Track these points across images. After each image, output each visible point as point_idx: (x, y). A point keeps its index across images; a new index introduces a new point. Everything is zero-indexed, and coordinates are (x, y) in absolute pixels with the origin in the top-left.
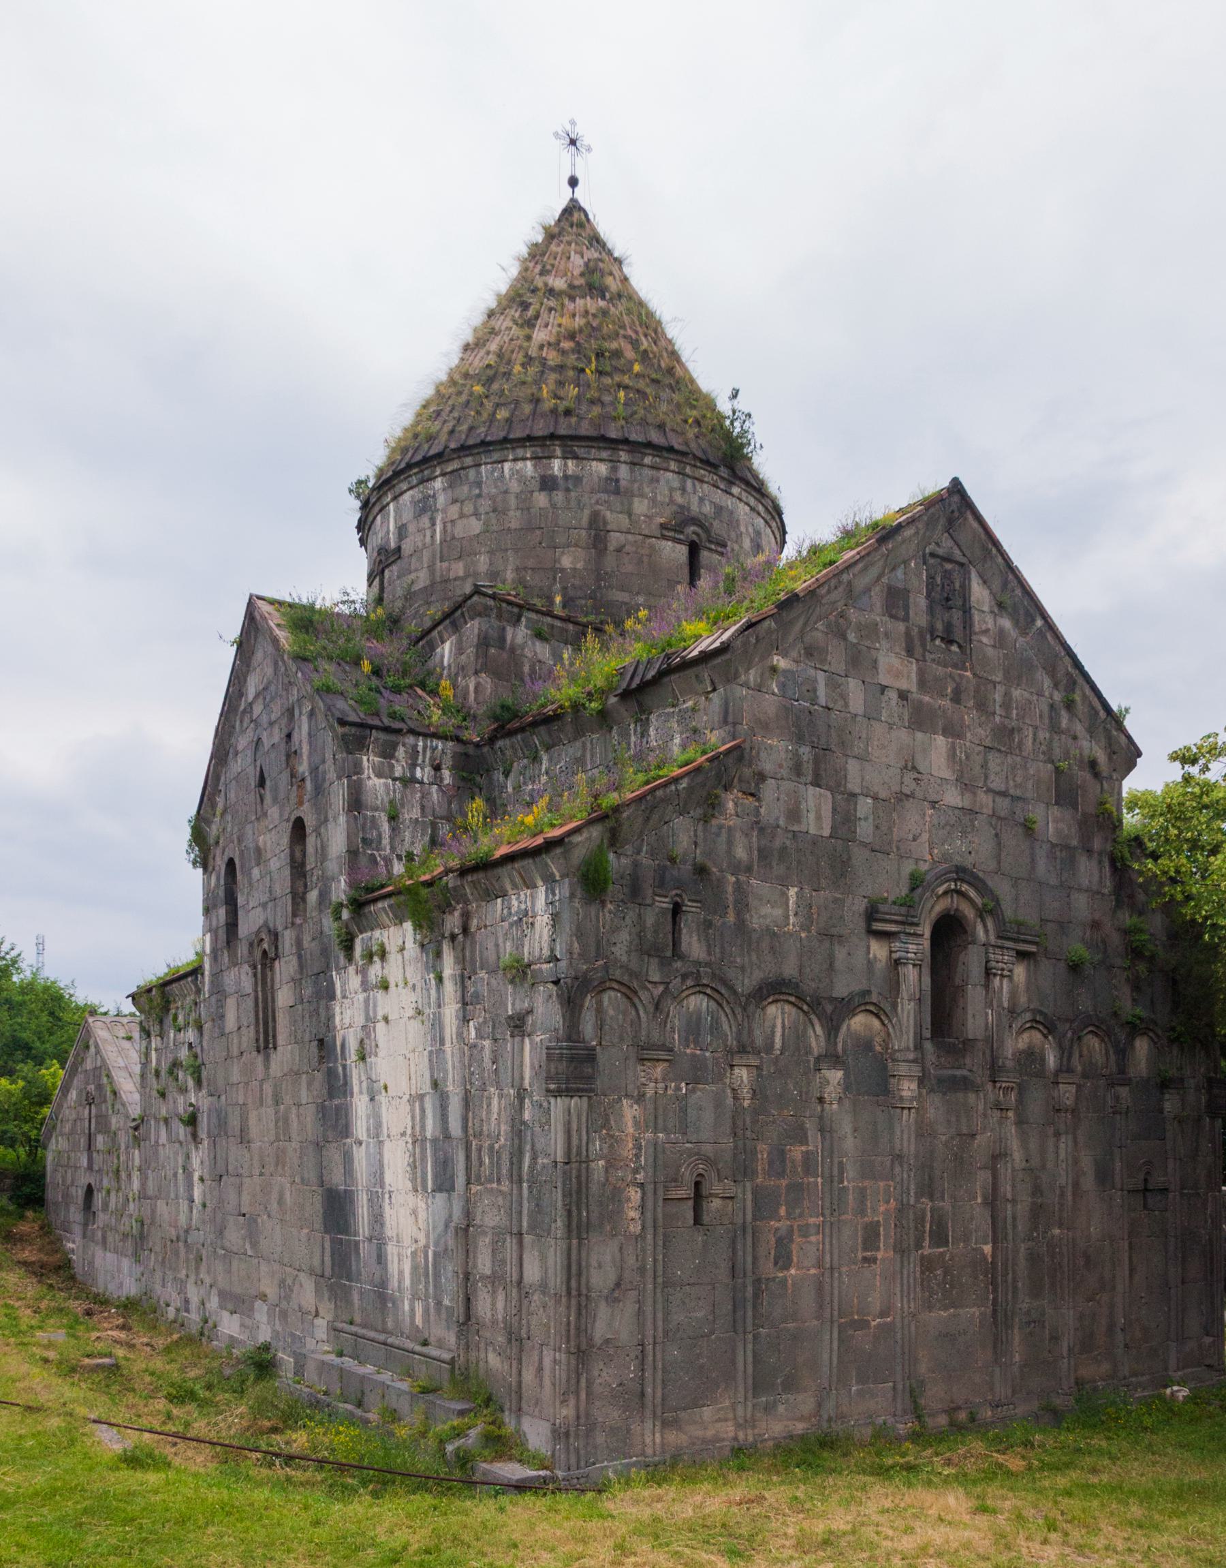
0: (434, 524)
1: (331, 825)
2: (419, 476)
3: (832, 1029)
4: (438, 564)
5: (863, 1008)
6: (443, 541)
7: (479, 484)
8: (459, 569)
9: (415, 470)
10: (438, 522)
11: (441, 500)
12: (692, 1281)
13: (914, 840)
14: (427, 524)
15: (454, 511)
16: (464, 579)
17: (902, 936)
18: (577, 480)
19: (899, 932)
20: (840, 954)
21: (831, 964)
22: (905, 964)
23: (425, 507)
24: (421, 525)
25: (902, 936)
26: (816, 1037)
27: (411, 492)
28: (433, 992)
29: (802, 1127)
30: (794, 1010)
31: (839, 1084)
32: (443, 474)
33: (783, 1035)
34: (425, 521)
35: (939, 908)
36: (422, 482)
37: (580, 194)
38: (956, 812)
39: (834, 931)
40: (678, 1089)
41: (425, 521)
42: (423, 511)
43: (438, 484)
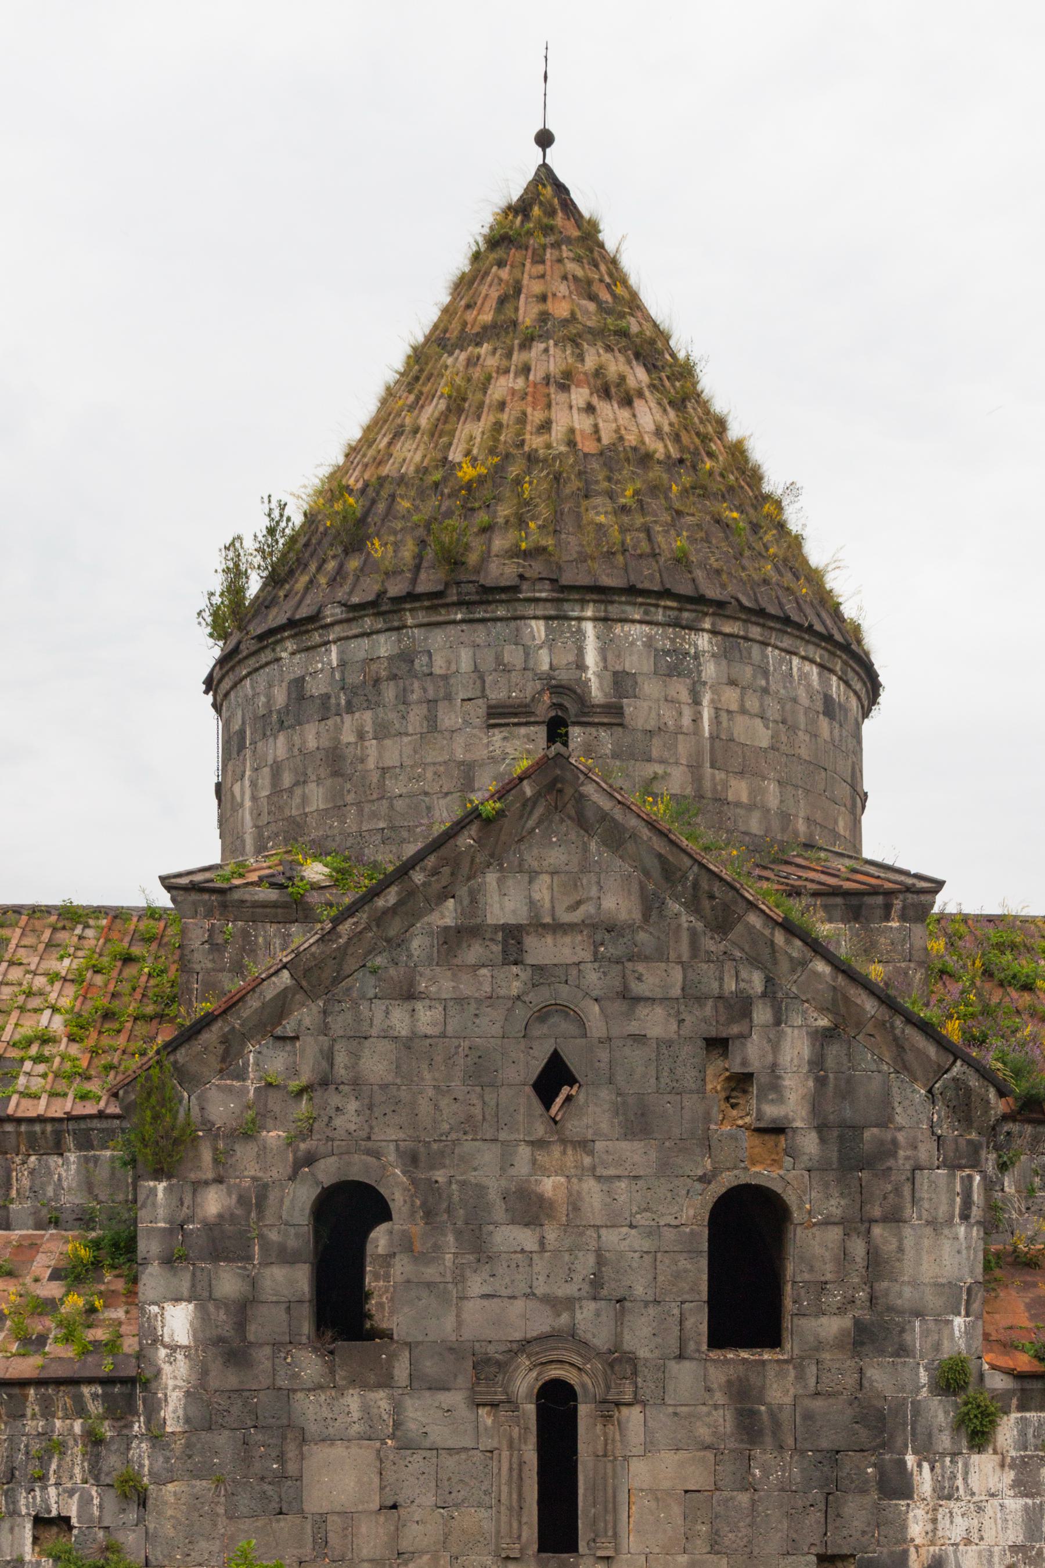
0: (697, 702)
2: (673, 614)
4: (708, 770)
6: (712, 738)
7: (766, 673)
8: (739, 790)
9: (669, 603)
10: (706, 702)
11: (710, 670)
14: (685, 696)
15: (731, 697)
16: (751, 807)
23: (676, 665)
24: (672, 693)
27: (646, 628)
32: (714, 632)
34: (680, 689)
36: (676, 624)
37: (557, 159)
42: (674, 671)
43: (703, 641)
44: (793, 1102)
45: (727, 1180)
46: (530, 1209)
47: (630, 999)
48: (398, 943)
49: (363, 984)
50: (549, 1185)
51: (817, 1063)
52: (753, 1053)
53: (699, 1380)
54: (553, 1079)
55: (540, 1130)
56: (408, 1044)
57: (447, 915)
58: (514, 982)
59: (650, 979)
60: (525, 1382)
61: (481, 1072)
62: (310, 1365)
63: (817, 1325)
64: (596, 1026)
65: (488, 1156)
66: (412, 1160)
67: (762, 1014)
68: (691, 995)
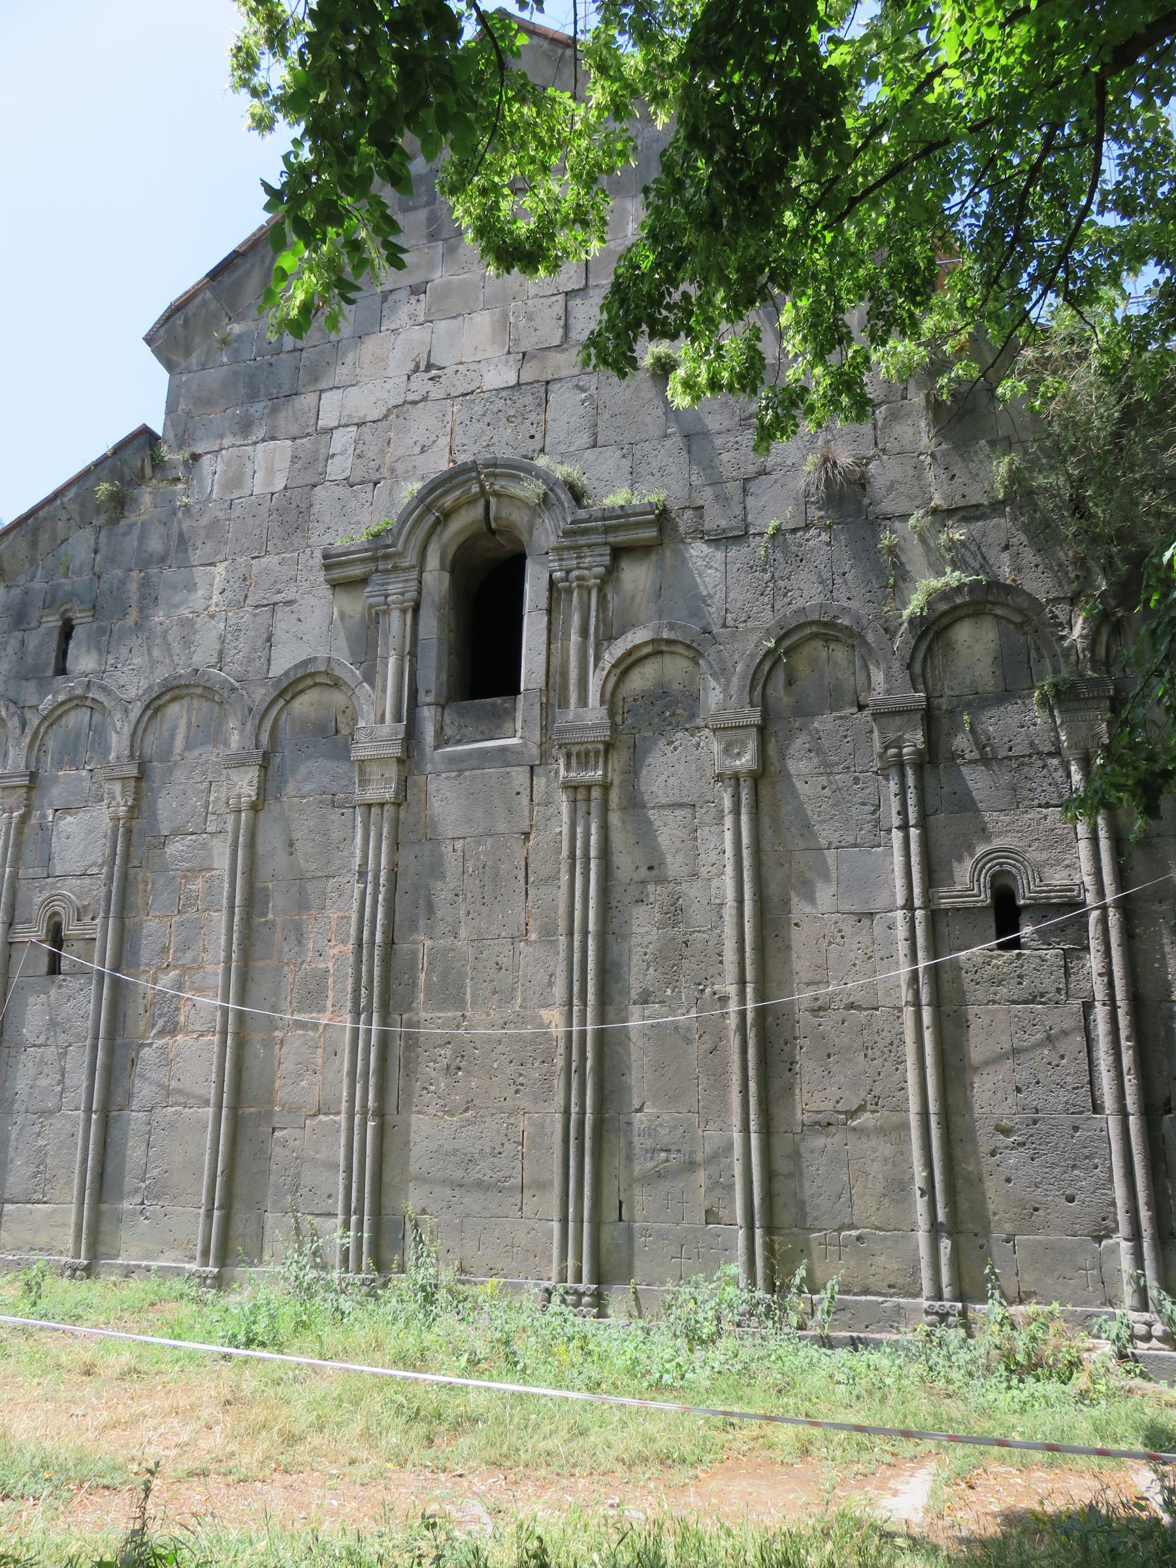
5: (310, 682)
12: (38, 1042)
13: (422, 451)
17: (375, 577)
19: (371, 573)
20: (284, 623)
21: (269, 640)
22: (384, 612)
25: (375, 577)
29: (204, 846)
30: (205, 705)
31: (250, 784)
33: (187, 737)
38: (503, 394)
39: (278, 598)
40: (44, 816)
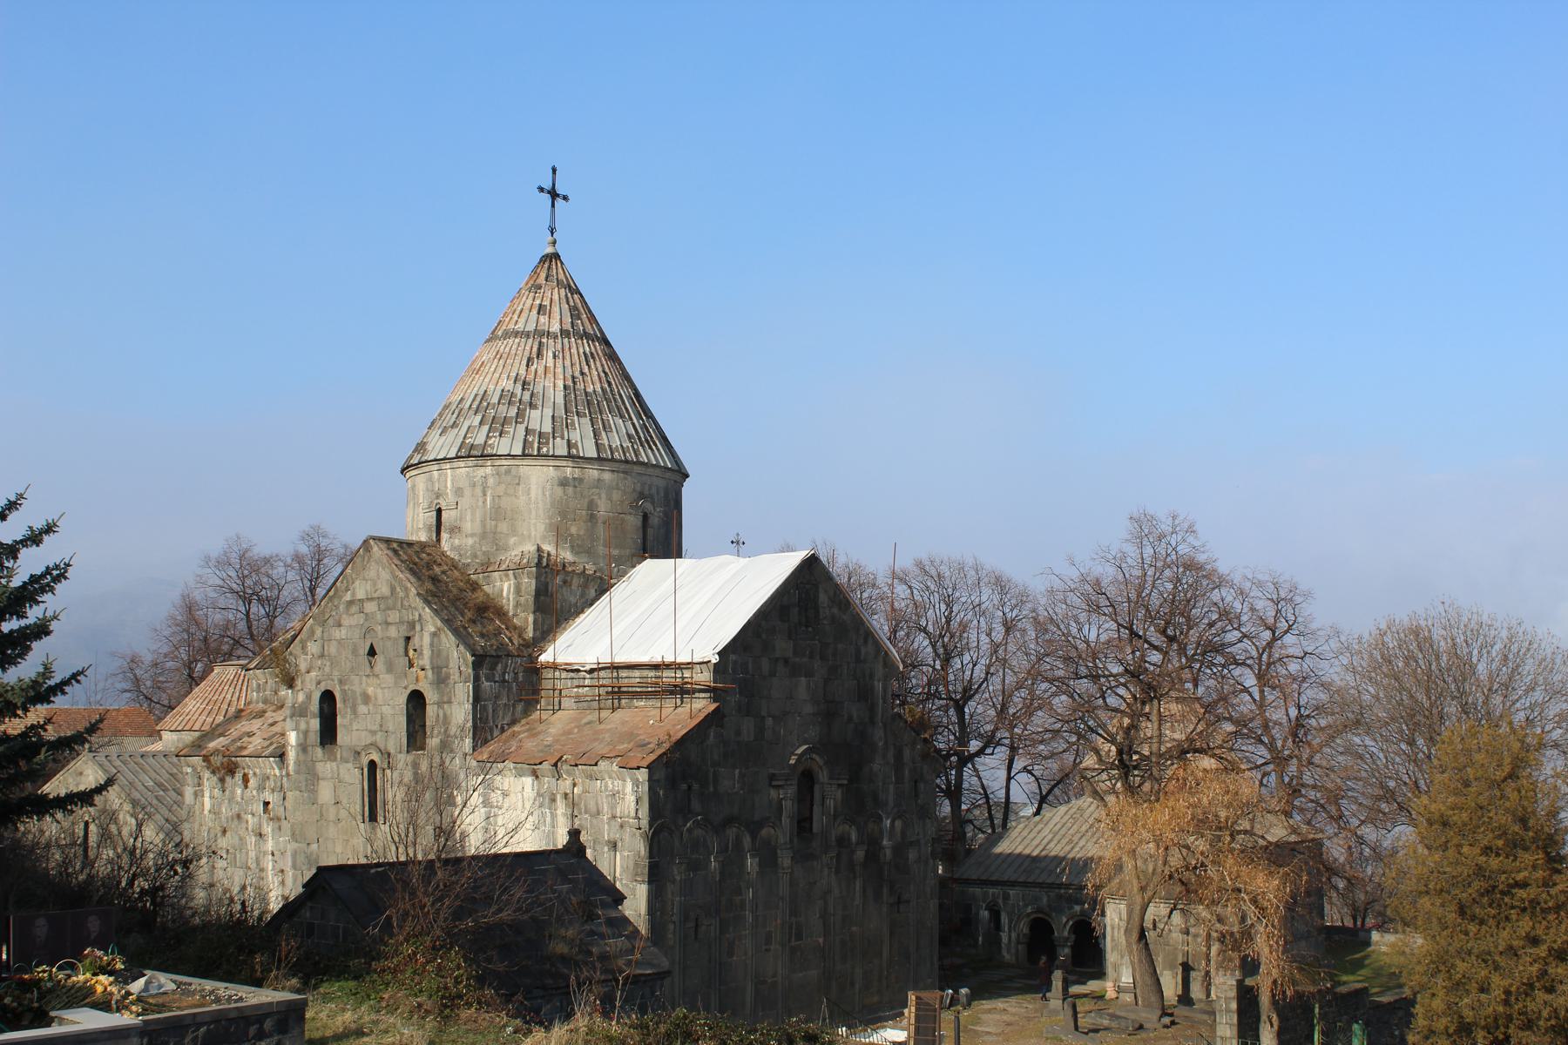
1: (455, 706)
3: (754, 838)
11: (491, 481)
15: (501, 490)
18: (580, 480)
26: (747, 841)
28: (548, 819)
35: (801, 769)
41: (478, 490)
43: (489, 470)
44: (426, 661)
45: (412, 687)
46: (366, 699)
47: (388, 624)
48: (337, 607)
49: (331, 621)
50: (370, 690)
51: (432, 645)
52: (415, 641)
53: (403, 759)
54: (372, 652)
55: (368, 671)
56: (339, 642)
57: (348, 597)
58: (360, 619)
59: (394, 616)
60: (365, 761)
61: (355, 652)
62: (319, 750)
63: (433, 742)
64: (380, 634)
65: (356, 679)
66: (341, 682)
67: (418, 628)
68: (401, 622)
